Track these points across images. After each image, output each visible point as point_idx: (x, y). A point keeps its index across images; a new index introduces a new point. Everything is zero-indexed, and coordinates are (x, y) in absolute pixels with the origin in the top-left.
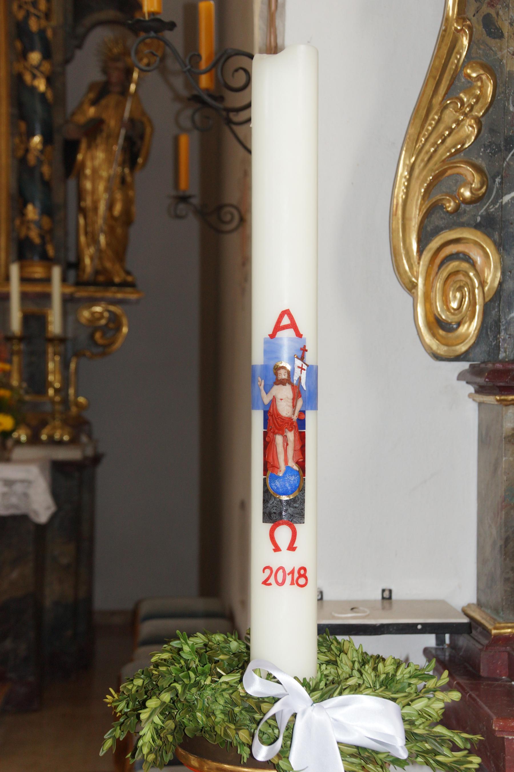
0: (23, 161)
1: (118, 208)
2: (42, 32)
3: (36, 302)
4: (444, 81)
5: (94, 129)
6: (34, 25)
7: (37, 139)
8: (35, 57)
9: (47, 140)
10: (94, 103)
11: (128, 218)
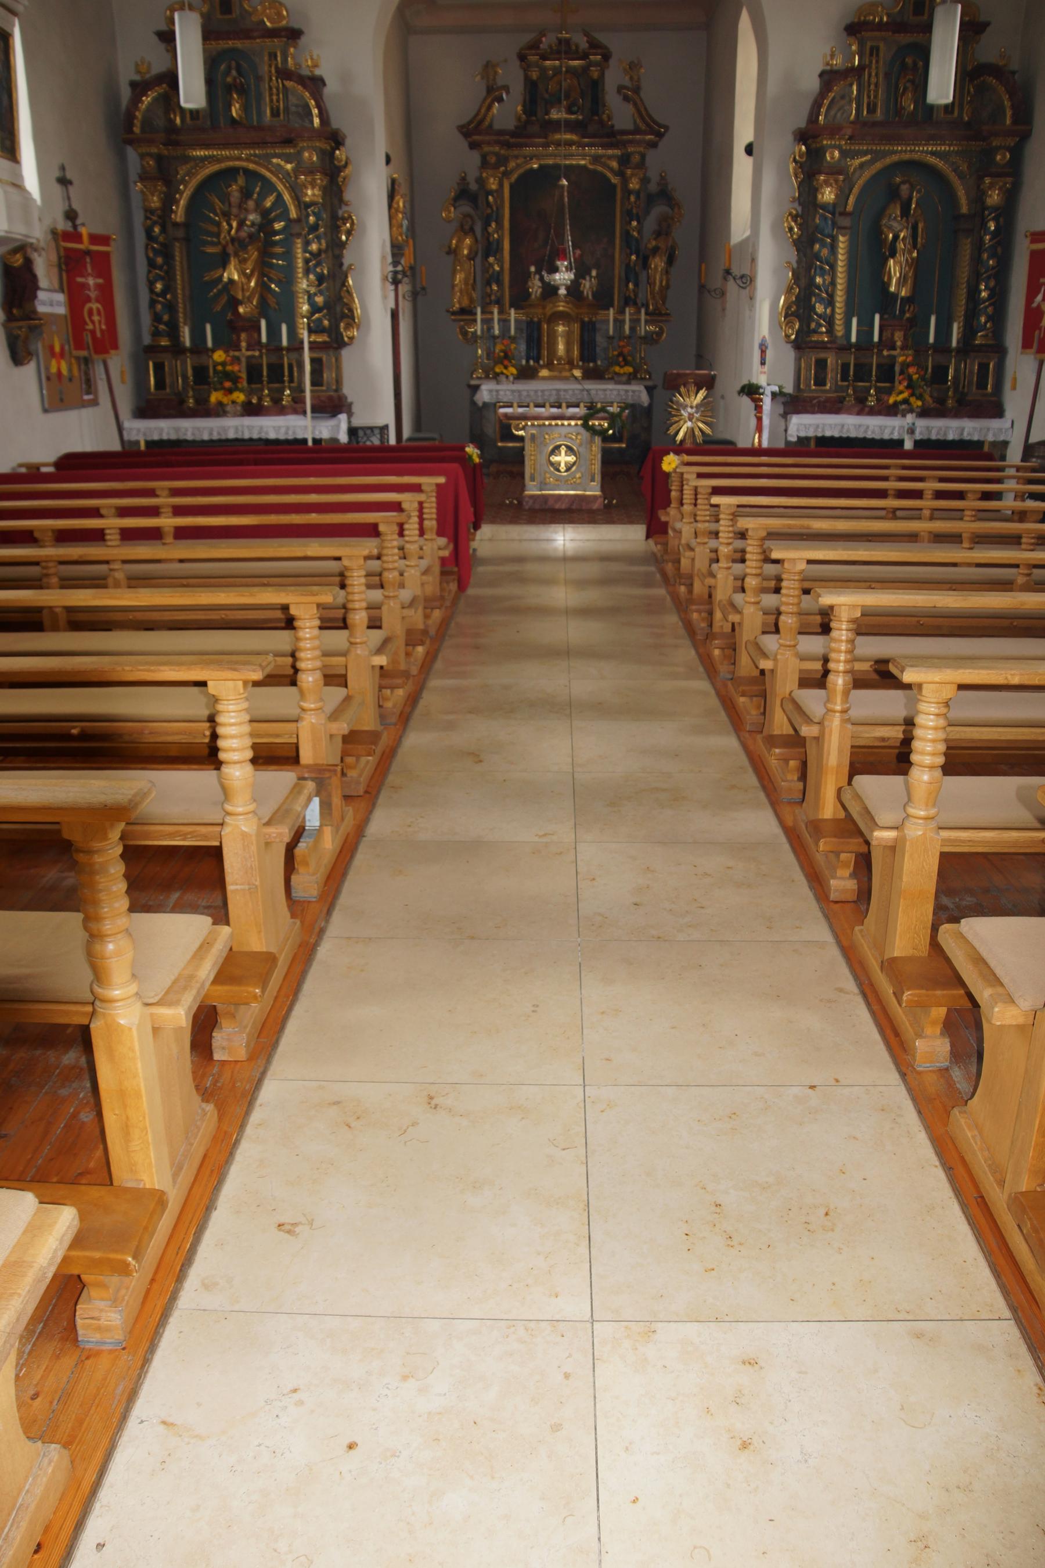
0: (628, 265)
1: (664, 283)
2: (637, 214)
3: (635, 322)
4: (789, 290)
5: (655, 250)
6: (634, 211)
7: (633, 257)
8: (634, 223)
9: (637, 257)
10: (655, 239)
11: (668, 286)
